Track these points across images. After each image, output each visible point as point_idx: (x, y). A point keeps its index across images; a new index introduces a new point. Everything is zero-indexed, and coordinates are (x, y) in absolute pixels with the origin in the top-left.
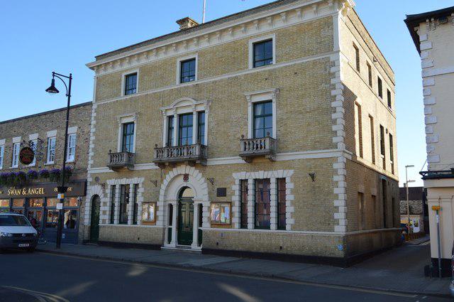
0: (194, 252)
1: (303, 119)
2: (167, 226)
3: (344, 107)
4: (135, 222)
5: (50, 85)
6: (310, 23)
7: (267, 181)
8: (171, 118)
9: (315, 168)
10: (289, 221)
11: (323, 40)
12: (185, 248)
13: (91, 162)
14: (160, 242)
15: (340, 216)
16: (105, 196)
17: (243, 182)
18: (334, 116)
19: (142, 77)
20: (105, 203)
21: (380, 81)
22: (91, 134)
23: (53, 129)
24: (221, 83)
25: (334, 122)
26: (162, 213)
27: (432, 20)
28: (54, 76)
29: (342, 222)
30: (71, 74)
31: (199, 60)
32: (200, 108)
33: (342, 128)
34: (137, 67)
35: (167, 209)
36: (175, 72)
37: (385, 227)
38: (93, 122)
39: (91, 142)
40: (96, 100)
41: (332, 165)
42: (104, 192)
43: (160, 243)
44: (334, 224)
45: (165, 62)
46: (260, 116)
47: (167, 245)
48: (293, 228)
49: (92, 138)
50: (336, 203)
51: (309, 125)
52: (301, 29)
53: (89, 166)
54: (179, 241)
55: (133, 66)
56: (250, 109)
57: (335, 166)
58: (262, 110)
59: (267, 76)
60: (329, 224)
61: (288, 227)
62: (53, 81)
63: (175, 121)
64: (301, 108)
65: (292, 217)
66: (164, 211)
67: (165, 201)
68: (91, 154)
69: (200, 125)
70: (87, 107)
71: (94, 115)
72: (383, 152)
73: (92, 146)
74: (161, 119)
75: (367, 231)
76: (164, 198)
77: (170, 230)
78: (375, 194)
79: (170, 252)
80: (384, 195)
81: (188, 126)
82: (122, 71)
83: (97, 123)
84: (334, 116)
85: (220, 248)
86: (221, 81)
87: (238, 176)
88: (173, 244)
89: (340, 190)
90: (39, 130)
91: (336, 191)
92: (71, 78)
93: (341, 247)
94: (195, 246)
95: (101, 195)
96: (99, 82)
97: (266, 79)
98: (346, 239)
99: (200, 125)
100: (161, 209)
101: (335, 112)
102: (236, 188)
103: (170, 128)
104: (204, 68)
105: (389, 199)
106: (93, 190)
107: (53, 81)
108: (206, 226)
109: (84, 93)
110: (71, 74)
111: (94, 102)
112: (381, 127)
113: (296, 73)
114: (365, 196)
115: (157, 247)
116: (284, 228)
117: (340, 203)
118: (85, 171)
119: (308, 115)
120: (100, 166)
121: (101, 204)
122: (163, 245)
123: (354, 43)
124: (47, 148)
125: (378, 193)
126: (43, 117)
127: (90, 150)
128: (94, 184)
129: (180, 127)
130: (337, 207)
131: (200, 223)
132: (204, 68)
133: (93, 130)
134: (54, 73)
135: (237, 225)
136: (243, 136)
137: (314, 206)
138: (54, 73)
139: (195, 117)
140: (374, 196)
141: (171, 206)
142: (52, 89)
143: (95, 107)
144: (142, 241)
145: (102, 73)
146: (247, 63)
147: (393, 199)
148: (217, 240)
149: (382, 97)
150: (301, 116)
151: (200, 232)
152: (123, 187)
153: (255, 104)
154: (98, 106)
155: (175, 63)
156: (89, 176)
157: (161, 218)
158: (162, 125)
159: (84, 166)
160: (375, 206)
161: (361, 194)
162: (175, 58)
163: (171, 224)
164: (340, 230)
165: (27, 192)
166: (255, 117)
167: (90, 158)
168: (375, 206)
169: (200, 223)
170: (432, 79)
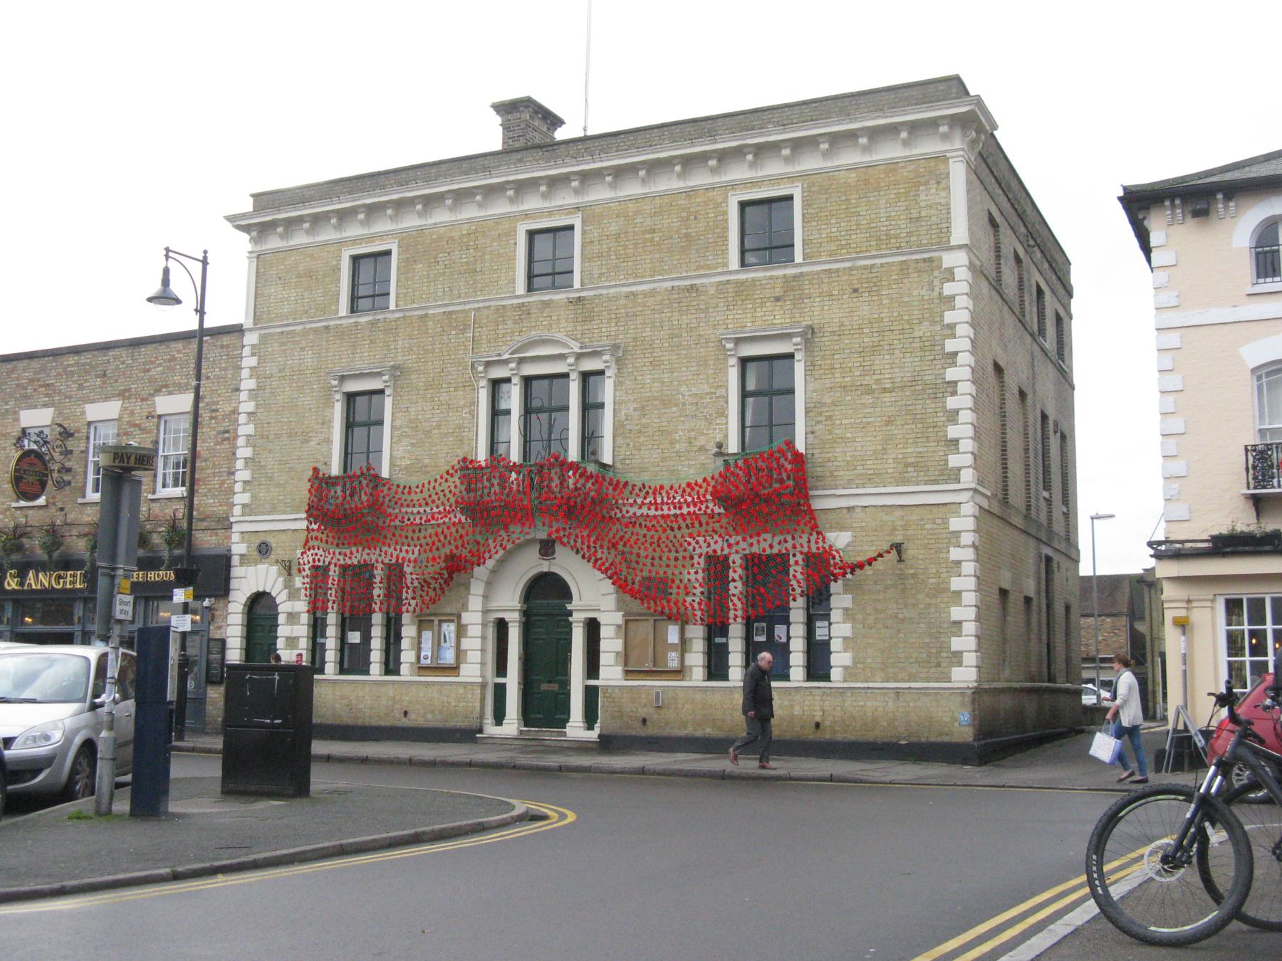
1: (873, 406)
2: (492, 679)
3: (974, 382)
4: (391, 666)
5: (156, 287)
6: (892, 166)
7: (781, 561)
8: (496, 384)
9: (905, 527)
10: (840, 659)
11: (923, 214)
12: (548, 734)
13: (241, 498)
14: (475, 724)
15: (965, 643)
16: (293, 596)
17: (717, 567)
18: (952, 402)
19: (407, 265)
20: (293, 618)
21: (1040, 292)
22: (242, 419)
23: (107, 399)
24: (650, 301)
25: (953, 416)
26: (477, 643)
27: (1177, 202)
28: (167, 257)
29: (970, 659)
30: (205, 252)
31: (584, 232)
32: (590, 365)
33: (970, 431)
34: (392, 234)
35: (491, 632)
36: (512, 259)
37: (1051, 679)
38: (248, 384)
39: (241, 442)
40: (256, 319)
41: (946, 521)
42: (288, 585)
43: (475, 724)
44: (951, 664)
45: (478, 229)
46: (753, 394)
47: (491, 729)
48: (849, 672)
49: (246, 429)
50: (956, 613)
51: (889, 422)
52: (867, 179)
53: (237, 510)
54: (527, 716)
55: (381, 233)
56: (733, 374)
57: (955, 524)
58: (767, 383)
59: (778, 292)
60: (938, 665)
61: (836, 674)
62: (166, 271)
63: (513, 399)
64: (868, 380)
65: (845, 650)
66: (483, 638)
67: (485, 612)
68: (243, 475)
69: (590, 407)
70: (226, 340)
71: (249, 361)
72: (1047, 486)
73: (244, 452)
74: (471, 387)
75: (1017, 685)
76: (484, 604)
77: (500, 691)
78: (1031, 594)
80: (1047, 597)
81: (550, 410)
82: (342, 243)
83: (259, 388)
84: (952, 402)
85: (650, 731)
86: (653, 293)
87: (703, 546)
88: (512, 725)
89: (965, 583)
90: (50, 395)
91: (955, 584)
92: (205, 262)
93: (965, 716)
94: (576, 728)
95: (281, 597)
96: (263, 267)
97: (778, 299)
98: (978, 692)
99: (590, 407)
100: (474, 630)
101: (954, 393)
102: (695, 575)
103: (497, 414)
104: (600, 256)
105: (1059, 609)
106: (248, 579)
107: (166, 271)
108: (611, 673)
109: (230, 306)
110: (205, 252)
111: (248, 324)
112: (1044, 417)
113: (856, 290)
114: (1012, 597)
115: (469, 735)
116: (827, 678)
117: (965, 612)
118: (225, 524)
119: (887, 398)
120: (273, 510)
121: (281, 619)
122: (481, 731)
123: (990, 213)
124: (86, 452)
125: (1038, 592)
126: (71, 360)
127: (239, 464)
128: (256, 563)
129: (528, 411)
130: (958, 624)
131: (592, 667)
132: (600, 256)
133: (247, 406)
134: (167, 250)
135: (698, 674)
136: (720, 446)
137: (903, 620)
138: (167, 250)
139: (574, 387)
140: (1028, 600)
141: (502, 626)
142: (165, 297)
143: (251, 339)
144: (416, 720)
145: (274, 243)
146: (725, 252)
147: (1068, 608)
148: (643, 712)
149: (1044, 337)
150: (868, 399)
151: (591, 695)
152: (350, 572)
153: (744, 362)
154: (264, 339)
155: (512, 233)
156: (236, 537)
157: (474, 656)
158: (474, 404)
159: (221, 510)
160: (1028, 623)
161: (1004, 593)
162: (513, 218)
163: (501, 669)
164: (965, 675)
165: (22, 584)
166: (744, 394)
167: (238, 487)
168: (1028, 623)
169: (592, 667)
170: (1177, 334)
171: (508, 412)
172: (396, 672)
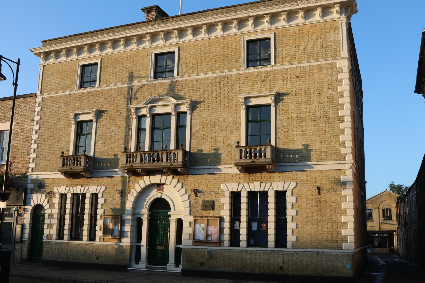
0: (172, 275)
7: (264, 194)
9: (321, 180)
12: (159, 268)
16: (51, 206)
17: (235, 197)
18: (341, 125)
20: (51, 216)
24: (206, 82)
25: (342, 132)
30: (19, 59)
35: (135, 223)
38: (37, 118)
49: (35, 137)
50: (344, 219)
51: (314, 134)
59: (263, 78)
63: (147, 123)
64: (304, 115)
70: (29, 100)
79: (140, 273)
84: (341, 125)
85: (204, 268)
86: (208, 79)
88: (142, 265)
92: (18, 64)
93: (349, 266)
94: (171, 267)
97: (263, 81)
101: (343, 121)
103: (140, 130)
110: (19, 59)
113: (298, 77)
119: (313, 123)
122: (130, 266)
129: (153, 129)
135: (226, 243)
137: (320, 221)
143: (39, 99)
144: (102, 261)
148: (201, 260)
150: (304, 124)
151: (178, 251)
159: (24, 171)
171: (145, 129)
172: (94, 240)
